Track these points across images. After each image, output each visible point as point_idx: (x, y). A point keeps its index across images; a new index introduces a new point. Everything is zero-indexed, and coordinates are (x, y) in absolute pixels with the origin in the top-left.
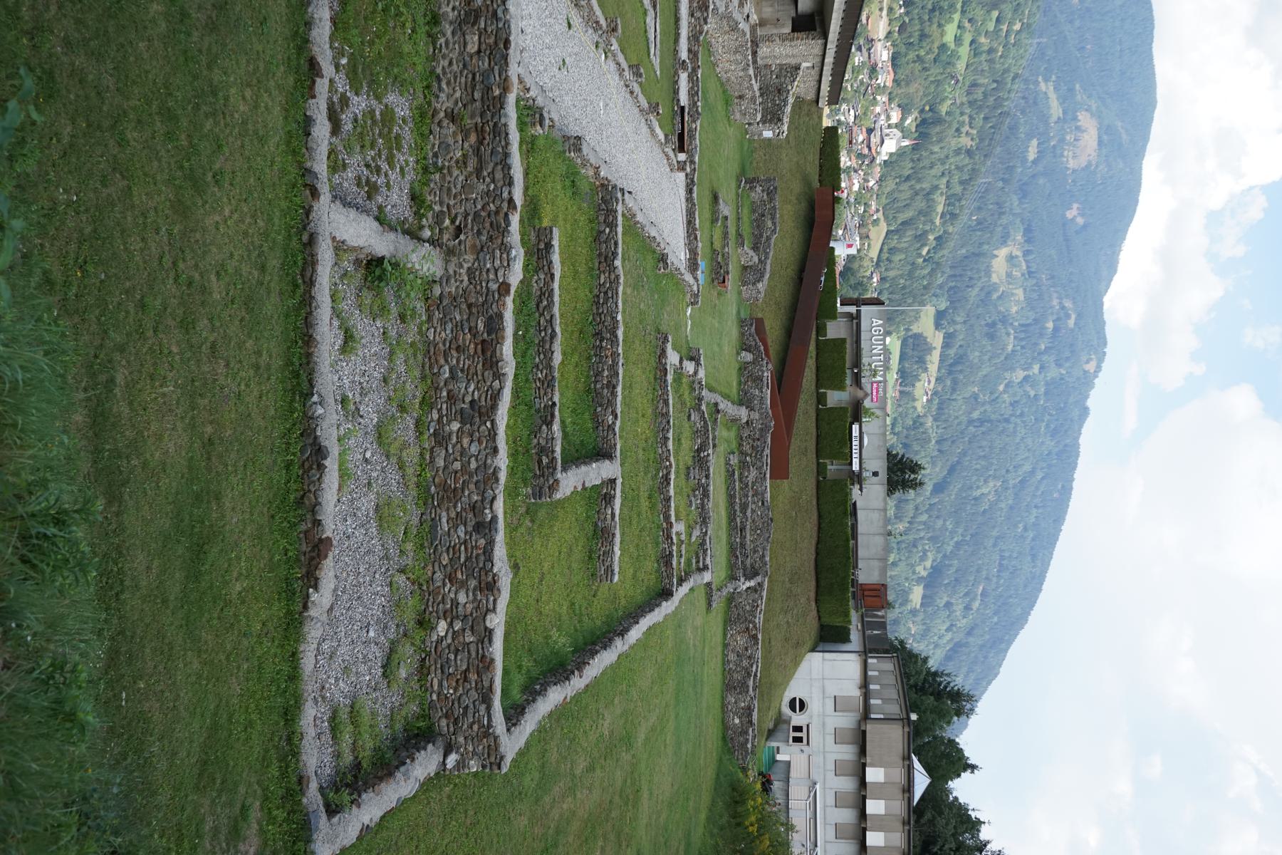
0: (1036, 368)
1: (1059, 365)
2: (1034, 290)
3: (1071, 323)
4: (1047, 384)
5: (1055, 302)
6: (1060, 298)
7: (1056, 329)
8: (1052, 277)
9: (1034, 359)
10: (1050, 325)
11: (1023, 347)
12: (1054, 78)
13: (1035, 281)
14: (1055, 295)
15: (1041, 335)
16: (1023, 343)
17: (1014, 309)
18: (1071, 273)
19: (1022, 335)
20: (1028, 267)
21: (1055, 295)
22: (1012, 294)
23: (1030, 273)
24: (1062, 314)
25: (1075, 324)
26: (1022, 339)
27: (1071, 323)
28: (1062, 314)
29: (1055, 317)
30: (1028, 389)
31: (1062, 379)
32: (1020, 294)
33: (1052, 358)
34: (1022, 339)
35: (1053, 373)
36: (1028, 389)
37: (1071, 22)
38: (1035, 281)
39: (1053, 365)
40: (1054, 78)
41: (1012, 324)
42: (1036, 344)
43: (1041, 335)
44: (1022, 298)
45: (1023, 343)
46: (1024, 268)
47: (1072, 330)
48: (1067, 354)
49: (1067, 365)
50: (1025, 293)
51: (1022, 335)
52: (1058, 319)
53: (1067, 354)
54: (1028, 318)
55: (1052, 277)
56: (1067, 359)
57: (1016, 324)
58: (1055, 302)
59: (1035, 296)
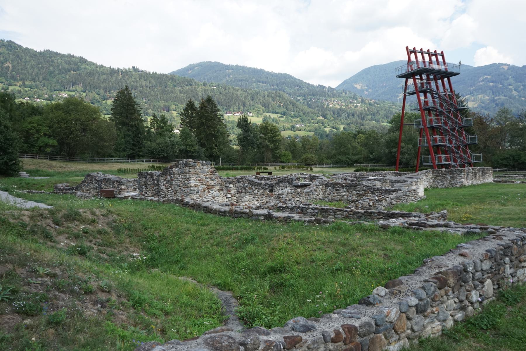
0: (510, 87)
1: (508, 79)
2: (478, 91)
3: (489, 77)
4: (517, 82)
5: (481, 83)
6: (479, 82)
7: (493, 82)
8: (471, 85)
9: (507, 88)
10: (491, 84)
11: (503, 93)
12: (397, 94)
13: (474, 92)
14: (478, 84)
15: (496, 87)
16: (501, 93)
17: (487, 97)
18: (468, 79)
19: (497, 94)
20: (468, 95)
21: (478, 84)
22: (481, 99)
23: (471, 94)
24: (486, 81)
25: (489, 75)
26: (499, 93)
27: (489, 77)
28: (486, 81)
29: (488, 83)
30: (520, 89)
31: (514, 77)
32: (480, 96)
33: (506, 82)
34: (499, 93)
35: (511, 80)
36: (520, 89)
37: (377, 91)
38: (474, 92)
39: (508, 81)
40: (397, 94)
41: (493, 98)
42: (500, 88)
43: (496, 87)
44: (482, 95)
45: (501, 93)
46: (469, 96)
47: (492, 76)
48: (503, 76)
49: (507, 76)
50: (479, 95)
51: (497, 94)
52: (488, 81)
53: (503, 76)
54: (490, 93)
55: (471, 85)
56: (505, 76)
57: (493, 96)
58: (481, 83)
59: (480, 91)
